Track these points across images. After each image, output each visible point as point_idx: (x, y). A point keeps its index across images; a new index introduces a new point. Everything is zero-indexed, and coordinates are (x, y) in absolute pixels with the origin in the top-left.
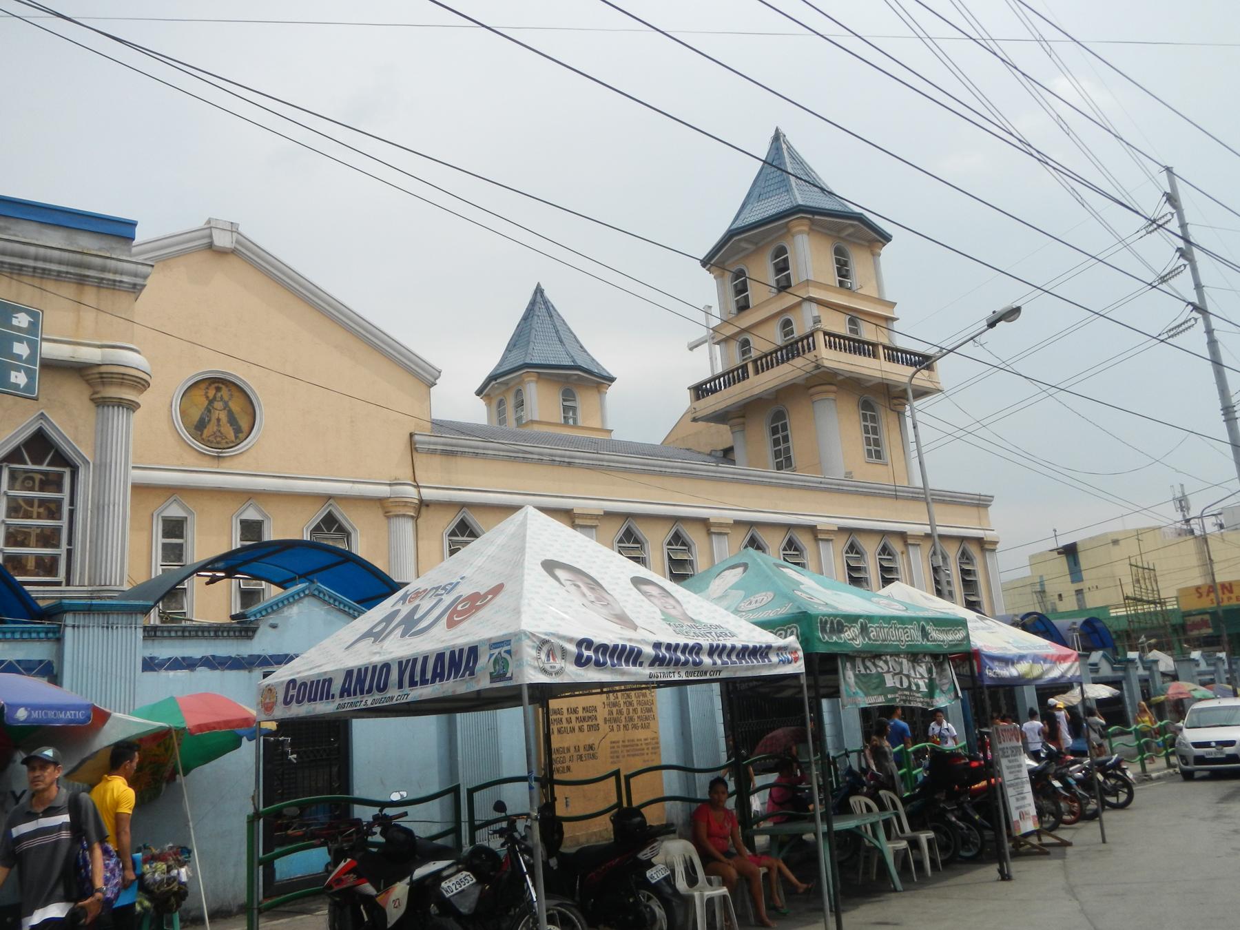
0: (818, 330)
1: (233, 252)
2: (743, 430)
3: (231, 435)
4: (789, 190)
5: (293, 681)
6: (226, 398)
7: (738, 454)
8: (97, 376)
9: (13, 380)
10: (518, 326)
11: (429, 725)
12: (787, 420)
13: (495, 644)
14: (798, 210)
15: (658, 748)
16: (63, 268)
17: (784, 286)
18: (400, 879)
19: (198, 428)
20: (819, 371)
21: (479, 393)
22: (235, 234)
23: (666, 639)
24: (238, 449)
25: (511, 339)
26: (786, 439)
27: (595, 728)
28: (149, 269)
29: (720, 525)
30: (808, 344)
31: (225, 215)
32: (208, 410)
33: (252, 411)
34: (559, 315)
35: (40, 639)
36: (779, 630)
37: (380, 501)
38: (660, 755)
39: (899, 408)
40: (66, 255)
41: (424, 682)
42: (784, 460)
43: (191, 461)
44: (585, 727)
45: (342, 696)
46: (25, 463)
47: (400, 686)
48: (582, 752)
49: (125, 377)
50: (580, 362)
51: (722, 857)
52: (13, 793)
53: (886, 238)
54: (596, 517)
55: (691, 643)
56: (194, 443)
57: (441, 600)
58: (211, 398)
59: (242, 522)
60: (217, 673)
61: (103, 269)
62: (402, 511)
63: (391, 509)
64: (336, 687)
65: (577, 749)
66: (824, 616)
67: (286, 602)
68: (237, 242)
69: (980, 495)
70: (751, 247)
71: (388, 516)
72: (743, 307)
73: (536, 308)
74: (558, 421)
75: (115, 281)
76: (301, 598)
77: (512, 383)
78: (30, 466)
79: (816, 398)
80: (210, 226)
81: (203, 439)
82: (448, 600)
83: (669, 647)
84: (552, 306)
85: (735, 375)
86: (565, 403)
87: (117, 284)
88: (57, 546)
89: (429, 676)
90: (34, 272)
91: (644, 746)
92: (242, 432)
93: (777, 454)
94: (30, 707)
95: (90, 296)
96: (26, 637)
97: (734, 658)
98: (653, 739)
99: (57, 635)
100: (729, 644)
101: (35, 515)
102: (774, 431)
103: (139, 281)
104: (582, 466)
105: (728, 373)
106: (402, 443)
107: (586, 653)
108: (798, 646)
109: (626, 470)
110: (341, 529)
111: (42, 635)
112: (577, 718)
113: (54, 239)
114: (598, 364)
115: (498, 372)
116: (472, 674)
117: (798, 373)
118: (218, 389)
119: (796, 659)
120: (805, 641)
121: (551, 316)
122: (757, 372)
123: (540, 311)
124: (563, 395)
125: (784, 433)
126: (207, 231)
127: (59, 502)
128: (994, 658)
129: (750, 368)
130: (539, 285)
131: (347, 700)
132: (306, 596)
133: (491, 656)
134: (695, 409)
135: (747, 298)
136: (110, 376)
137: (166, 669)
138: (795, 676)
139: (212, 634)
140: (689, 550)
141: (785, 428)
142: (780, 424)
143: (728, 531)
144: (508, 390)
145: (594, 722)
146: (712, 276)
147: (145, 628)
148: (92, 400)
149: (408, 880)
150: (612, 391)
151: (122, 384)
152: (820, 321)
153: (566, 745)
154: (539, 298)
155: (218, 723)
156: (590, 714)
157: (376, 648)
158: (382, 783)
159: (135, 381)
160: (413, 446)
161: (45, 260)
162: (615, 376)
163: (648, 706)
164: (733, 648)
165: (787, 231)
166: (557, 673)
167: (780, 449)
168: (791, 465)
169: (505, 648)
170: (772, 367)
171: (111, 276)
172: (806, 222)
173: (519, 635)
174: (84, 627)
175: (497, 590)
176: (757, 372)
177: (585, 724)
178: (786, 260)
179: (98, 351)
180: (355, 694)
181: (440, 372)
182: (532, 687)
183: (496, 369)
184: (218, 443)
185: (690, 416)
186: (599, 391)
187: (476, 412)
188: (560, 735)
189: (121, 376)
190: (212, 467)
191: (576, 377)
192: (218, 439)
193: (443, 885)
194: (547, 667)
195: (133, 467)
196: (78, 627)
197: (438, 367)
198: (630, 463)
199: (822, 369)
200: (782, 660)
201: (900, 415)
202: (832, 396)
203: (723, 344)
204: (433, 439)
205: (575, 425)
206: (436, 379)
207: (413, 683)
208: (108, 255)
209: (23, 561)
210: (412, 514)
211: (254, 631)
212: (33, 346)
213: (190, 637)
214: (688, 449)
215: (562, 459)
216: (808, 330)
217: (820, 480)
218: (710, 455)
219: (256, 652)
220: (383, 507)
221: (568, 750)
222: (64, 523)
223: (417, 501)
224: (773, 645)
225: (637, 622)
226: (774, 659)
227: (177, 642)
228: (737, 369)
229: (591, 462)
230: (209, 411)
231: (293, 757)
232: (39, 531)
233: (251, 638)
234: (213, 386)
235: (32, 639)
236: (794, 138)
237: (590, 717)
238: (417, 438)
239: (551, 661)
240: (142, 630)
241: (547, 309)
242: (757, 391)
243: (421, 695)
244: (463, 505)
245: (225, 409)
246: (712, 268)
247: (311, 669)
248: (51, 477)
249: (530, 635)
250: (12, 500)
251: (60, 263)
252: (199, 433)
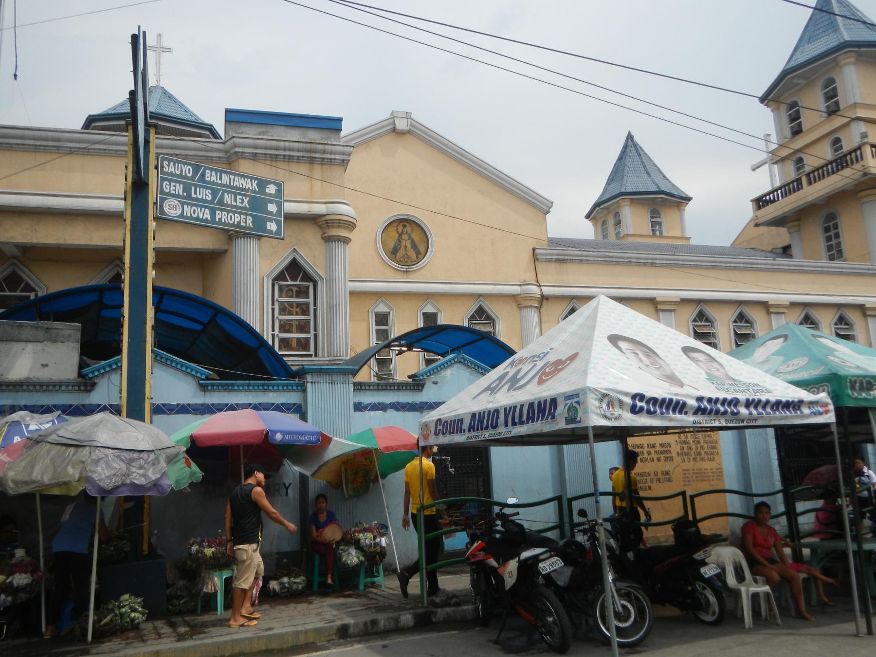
0: (865, 144)
1: (409, 132)
3: (414, 256)
4: (835, 29)
5: (440, 420)
6: (409, 232)
7: (795, 250)
8: (324, 222)
9: (269, 228)
10: (615, 165)
11: (543, 453)
12: (838, 221)
13: (569, 397)
14: (845, 45)
15: (722, 476)
16: (301, 154)
17: (833, 111)
18: (512, 558)
19: (393, 253)
20: (865, 178)
21: (588, 216)
22: (409, 120)
23: (707, 394)
24: (419, 266)
25: (610, 176)
26: (837, 236)
27: (671, 459)
28: (352, 149)
29: (778, 306)
30: (856, 156)
31: (401, 107)
33: (426, 239)
34: (646, 154)
35: (293, 390)
36: (812, 388)
37: (514, 297)
38: (723, 481)
40: (301, 145)
41: (521, 423)
42: (835, 252)
43: (390, 275)
44: (662, 458)
45: (469, 431)
46: (287, 281)
47: (506, 425)
48: (660, 476)
49: (341, 222)
50: (663, 188)
51: (766, 563)
52: (284, 484)
55: (729, 397)
56: (391, 263)
57: (535, 365)
58: (400, 232)
59: (425, 314)
60: (401, 413)
61: (324, 152)
62: (530, 303)
63: (522, 302)
64: (466, 425)
65: (656, 474)
66: (853, 376)
67: (442, 367)
68: (411, 125)
70: (802, 82)
71: (520, 307)
72: (797, 132)
73: (628, 150)
74: (648, 234)
75: (331, 159)
76: (452, 364)
77: (611, 209)
78: (290, 282)
79: (865, 200)
80: (393, 116)
81: (397, 260)
82: (540, 364)
83: (710, 400)
84: (640, 148)
85: (790, 188)
86: (653, 220)
87: (333, 161)
88: (308, 332)
89: (524, 418)
90: (284, 158)
91: (711, 475)
92: (421, 254)
93: (830, 248)
94: (284, 433)
95: (317, 171)
96: (286, 389)
97: (768, 410)
98: (718, 469)
99: (303, 388)
100: (764, 398)
101: (294, 313)
102: (827, 230)
103: (346, 157)
105: (784, 186)
106: (527, 256)
107: (639, 404)
108: (829, 401)
109: (697, 267)
111: (295, 388)
112: (655, 452)
113: (294, 135)
114: (677, 188)
115: (601, 200)
116: (553, 418)
117: (847, 181)
118: (404, 226)
119: (827, 412)
120: (836, 397)
121: (639, 155)
122: (810, 183)
123: (632, 152)
124: (651, 213)
125: (836, 231)
126: (392, 120)
127: (308, 304)
129: (804, 180)
130: (629, 133)
131: (473, 434)
132: (455, 362)
133: (566, 405)
134: (756, 216)
135: (800, 124)
136: (331, 221)
137: (369, 410)
138: (827, 425)
139: (396, 388)
140: (752, 326)
141: (836, 226)
142: (831, 224)
143: (785, 310)
144: (609, 213)
145: (669, 455)
146: (769, 109)
147: (354, 384)
148: (322, 238)
149: (517, 559)
150: (689, 208)
151: (339, 227)
152: (866, 136)
153: (647, 471)
154: (630, 143)
155: (399, 446)
156: (665, 449)
157: (491, 399)
158: (513, 490)
159: (346, 224)
160: (535, 257)
162: (690, 195)
163: (713, 445)
164: (768, 402)
165: (836, 64)
166: (616, 419)
167: (832, 245)
169: (575, 398)
170: (824, 177)
171: (328, 156)
172: (852, 54)
173: (585, 390)
174: (318, 383)
175: (573, 358)
176: (810, 183)
177: (662, 456)
178: (835, 89)
179: (324, 206)
180: (478, 430)
181: (552, 203)
182: (595, 428)
183: (599, 198)
184: (406, 262)
185: (752, 224)
187: (586, 231)
188: (642, 463)
189: (338, 221)
190: (403, 278)
191: (660, 199)
192: (406, 260)
193: (541, 565)
194: (608, 414)
195: (349, 281)
196: (315, 383)
197: (551, 199)
198: (701, 261)
199: (870, 176)
200: (813, 412)
203: (780, 164)
204: (549, 251)
205: (661, 236)
206: (550, 208)
207: (514, 424)
208: (326, 142)
209: (290, 342)
210: (536, 305)
211: (423, 386)
212: (279, 205)
213: (382, 390)
214: (752, 249)
215: (646, 261)
216: (855, 145)
217: (868, 267)
218: (771, 252)
219: (424, 400)
220: (516, 301)
221: (649, 474)
223: (539, 296)
224: (805, 400)
225: (684, 381)
226: (806, 411)
227: (375, 393)
228: (792, 182)
229: (668, 262)
230: (400, 241)
231: (452, 470)
232: (297, 323)
233: (421, 390)
234: (401, 224)
235: (289, 390)
237: (665, 451)
238: (538, 251)
239: (611, 409)
240: (352, 385)
241: (637, 150)
242: (810, 199)
243: (519, 433)
245: (409, 239)
246: (771, 103)
247: (451, 412)
248: (302, 289)
249: (594, 390)
250: (281, 304)
251: (299, 151)
252: (394, 256)
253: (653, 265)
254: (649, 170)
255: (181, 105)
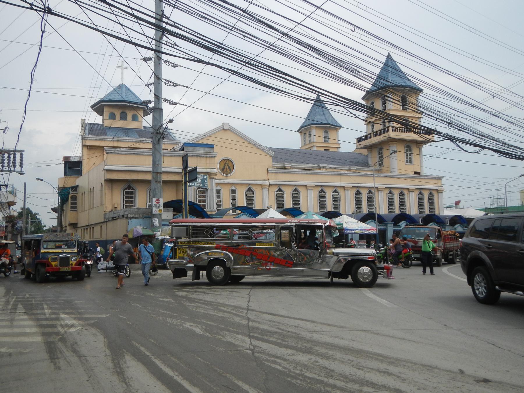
1: (229, 130)
2: (371, 153)
3: (229, 171)
21: (298, 131)
29: (348, 188)
32: (224, 166)
37: (261, 184)
39: (420, 147)
42: (381, 163)
53: (421, 91)
54: (313, 187)
58: (225, 163)
61: (210, 155)
62: (266, 187)
69: (438, 176)
77: (308, 129)
78: (201, 190)
79: (390, 146)
88: (205, 203)
95: (208, 159)
102: (379, 154)
103: (215, 156)
104: (309, 174)
110: (252, 191)
114: (336, 121)
117: (386, 138)
118: (226, 161)
126: (223, 126)
127: (205, 195)
128: (348, 230)
129: (372, 135)
141: (382, 154)
143: (350, 189)
150: (341, 131)
160: (268, 172)
161: (201, 154)
162: (342, 125)
168: (382, 165)
176: (374, 137)
179: (210, 169)
186: (337, 131)
201: (420, 149)
202: (395, 145)
203: (367, 125)
204: (272, 170)
220: (261, 186)
222: (206, 199)
236: (394, 57)
238: (269, 170)
242: (373, 142)
244: (279, 185)
250: (199, 195)
253: (306, 174)
254: (325, 113)
255: (134, 94)
